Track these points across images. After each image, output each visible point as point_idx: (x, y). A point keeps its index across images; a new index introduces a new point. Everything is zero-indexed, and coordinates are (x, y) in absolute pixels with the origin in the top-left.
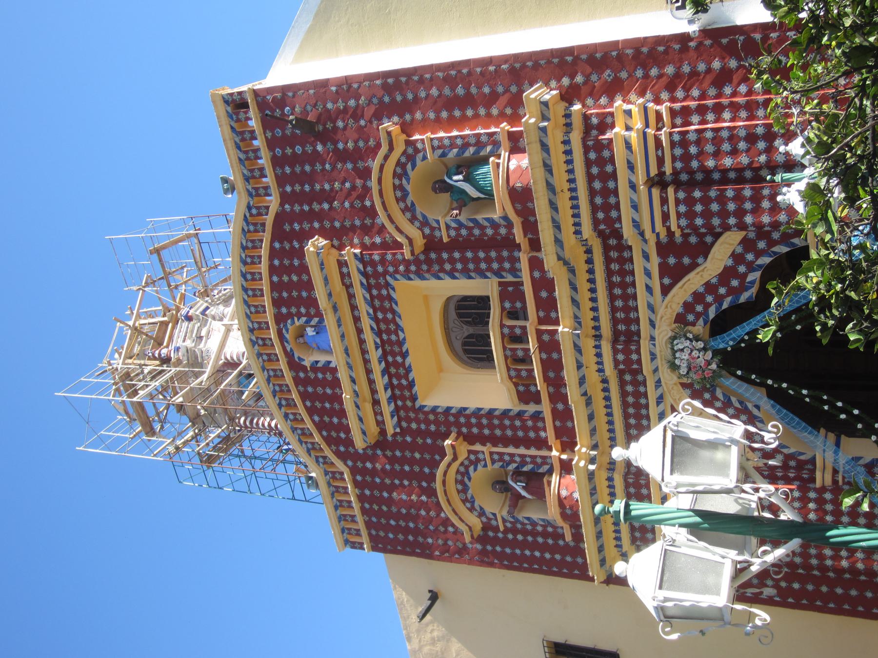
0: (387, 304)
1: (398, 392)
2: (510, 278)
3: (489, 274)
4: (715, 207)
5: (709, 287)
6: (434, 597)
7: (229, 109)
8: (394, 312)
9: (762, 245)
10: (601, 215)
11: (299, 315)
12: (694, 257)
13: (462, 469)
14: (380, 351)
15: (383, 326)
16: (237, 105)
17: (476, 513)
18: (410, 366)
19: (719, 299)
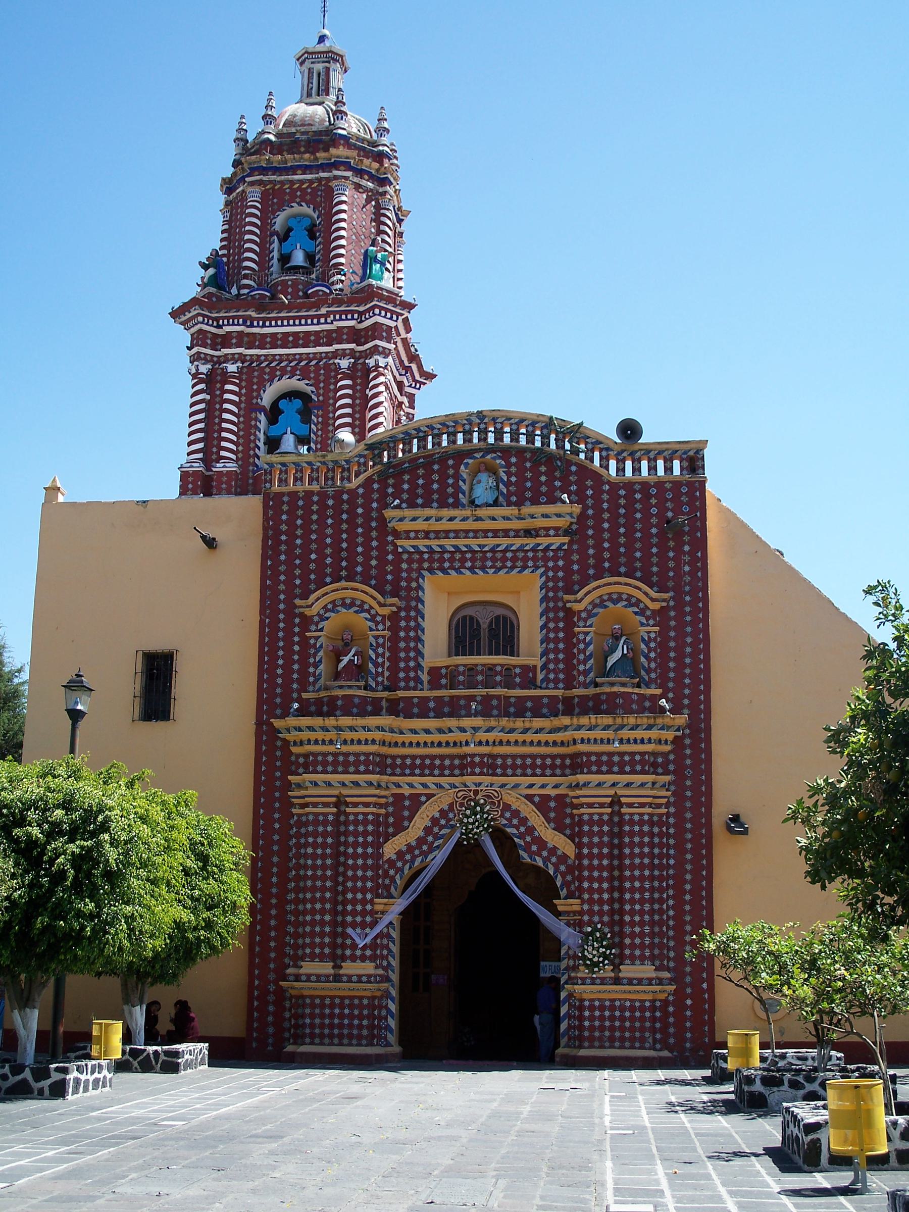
0: (519, 564)
1: (437, 556)
2: (540, 676)
3: (544, 659)
4: (596, 840)
5: (531, 830)
6: (210, 543)
7: (691, 453)
8: (513, 568)
9: (563, 868)
10: (593, 758)
12: (555, 820)
13: (366, 607)
14: (478, 549)
15: (499, 555)
16: (694, 459)
17: (322, 612)
18: (461, 573)
19: (521, 836)
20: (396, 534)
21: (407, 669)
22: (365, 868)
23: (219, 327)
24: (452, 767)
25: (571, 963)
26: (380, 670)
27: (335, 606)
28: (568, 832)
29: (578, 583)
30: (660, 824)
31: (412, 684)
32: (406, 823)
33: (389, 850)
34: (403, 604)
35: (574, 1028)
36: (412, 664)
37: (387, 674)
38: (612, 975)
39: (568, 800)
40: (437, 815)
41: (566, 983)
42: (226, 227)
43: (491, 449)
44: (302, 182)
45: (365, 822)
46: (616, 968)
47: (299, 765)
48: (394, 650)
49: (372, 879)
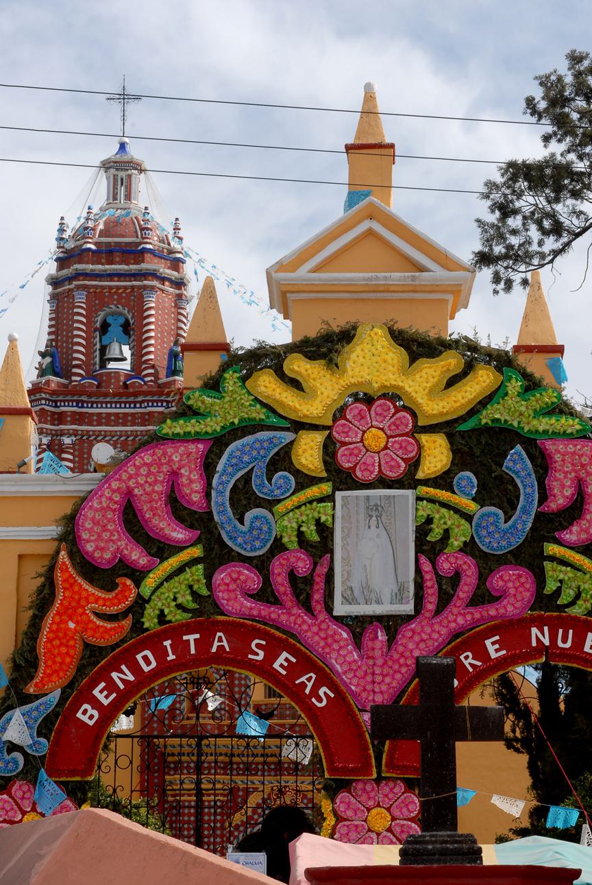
23: (56, 406)
42: (53, 316)
44: (118, 288)
45: (215, 807)
47: (170, 769)
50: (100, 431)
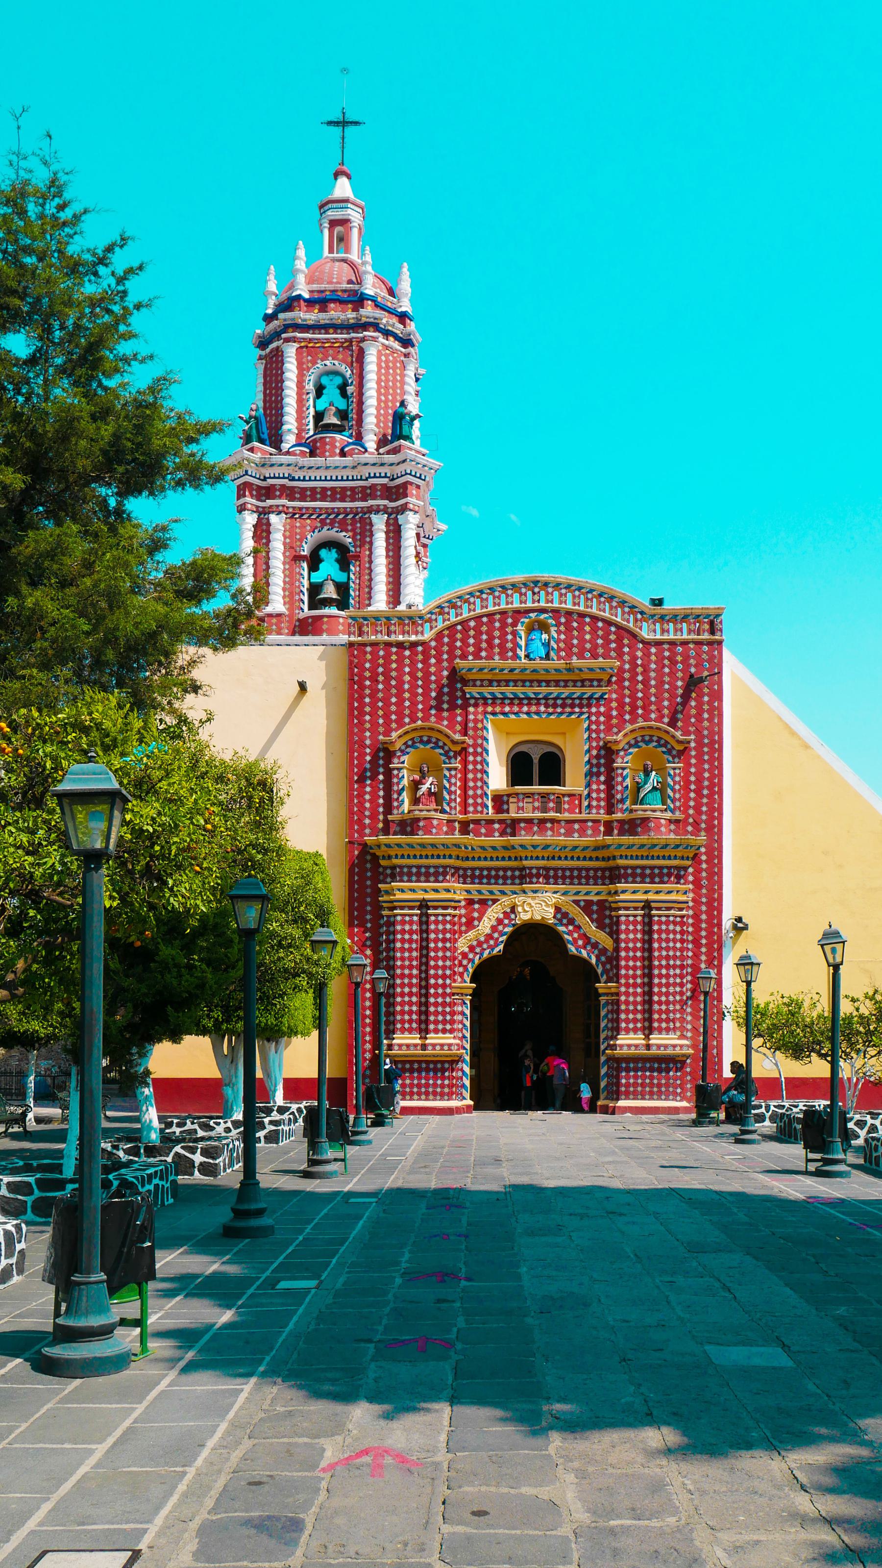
9: (603, 959)
10: (629, 871)
11: (559, 632)
13: (441, 744)
14: (533, 696)
17: (403, 748)
19: (570, 933)
20: (465, 682)
21: (475, 797)
22: (444, 958)
24: (513, 878)
25: (610, 1034)
26: (453, 797)
27: (414, 743)
28: (607, 930)
29: (616, 726)
30: (682, 924)
31: (479, 808)
32: (476, 923)
33: (462, 945)
34: (471, 742)
35: (612, 1084)
36: (479, 792)
37: (458, 800)
38: (644, 1042)
39: (607, 904)
40: (501, 916)
41: (606, 1049)
43: (543, 611)
46: (647, 1037)
47: (386, 876)
48: (465, 780)
49: (450, 968)
50: (314, 509)
